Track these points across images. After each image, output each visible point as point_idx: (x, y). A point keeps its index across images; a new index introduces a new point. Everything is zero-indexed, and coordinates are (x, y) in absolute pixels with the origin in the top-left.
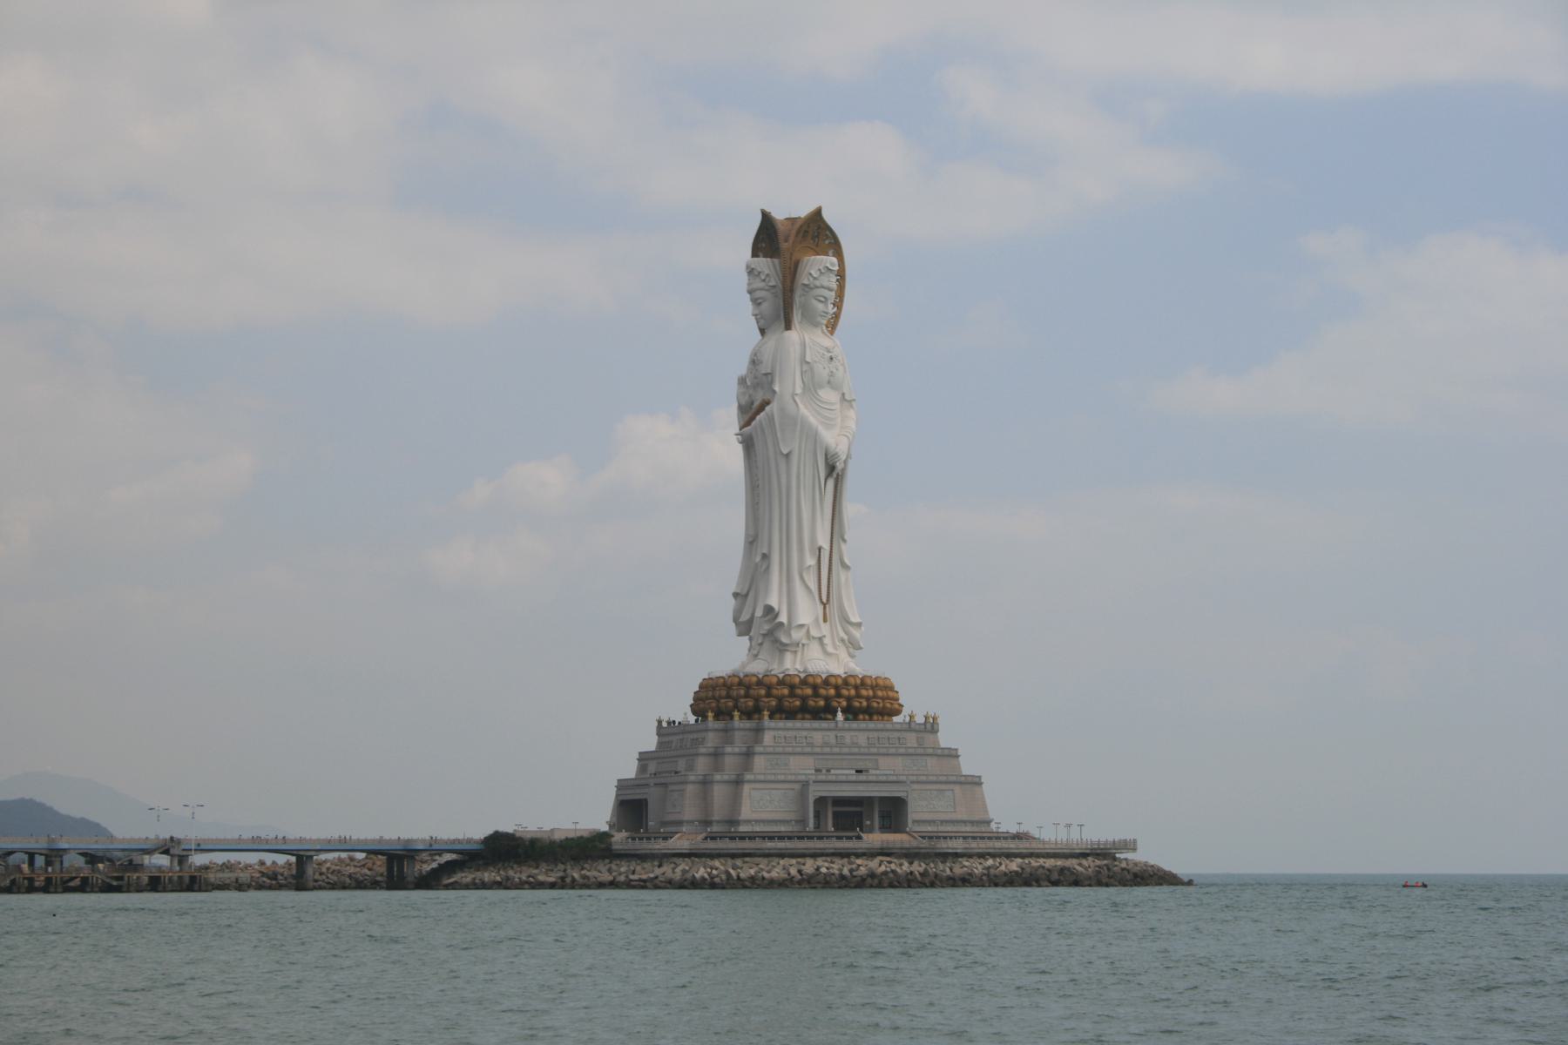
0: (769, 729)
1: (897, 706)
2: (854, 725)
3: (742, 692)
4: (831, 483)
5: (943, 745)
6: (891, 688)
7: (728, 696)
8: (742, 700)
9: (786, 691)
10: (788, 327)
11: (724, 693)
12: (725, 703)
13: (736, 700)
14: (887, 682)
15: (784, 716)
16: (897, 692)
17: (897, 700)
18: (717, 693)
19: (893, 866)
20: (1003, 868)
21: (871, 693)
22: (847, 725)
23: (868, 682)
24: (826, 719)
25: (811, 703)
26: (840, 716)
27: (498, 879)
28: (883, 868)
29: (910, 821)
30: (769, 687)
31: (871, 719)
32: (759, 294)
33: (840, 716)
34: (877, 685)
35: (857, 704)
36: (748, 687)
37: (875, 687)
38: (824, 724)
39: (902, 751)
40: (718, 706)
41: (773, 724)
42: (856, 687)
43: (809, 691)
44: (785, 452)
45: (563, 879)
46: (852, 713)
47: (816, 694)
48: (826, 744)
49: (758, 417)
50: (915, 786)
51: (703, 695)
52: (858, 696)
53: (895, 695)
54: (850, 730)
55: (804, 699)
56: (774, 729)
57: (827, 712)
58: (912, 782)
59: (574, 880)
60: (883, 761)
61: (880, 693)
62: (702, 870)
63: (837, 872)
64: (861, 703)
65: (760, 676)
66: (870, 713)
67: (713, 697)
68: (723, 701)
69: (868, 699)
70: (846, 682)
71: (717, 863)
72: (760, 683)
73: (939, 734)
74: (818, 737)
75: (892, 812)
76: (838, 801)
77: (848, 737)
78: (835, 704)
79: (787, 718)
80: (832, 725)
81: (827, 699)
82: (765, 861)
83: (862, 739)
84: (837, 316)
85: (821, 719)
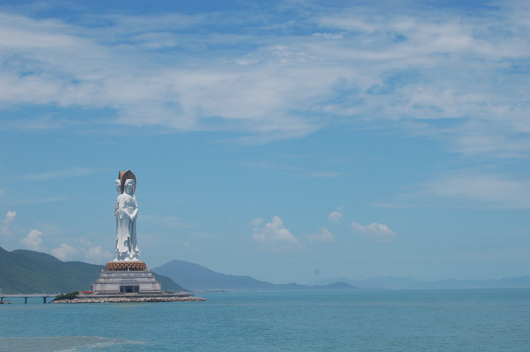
4: (131, 224)
8: (111, 267)
10: (122, 194)
13: (114, 267)
19: (125, 299)
20: (148, 300)
26: (128, 270)
27: (58, 302)
28: (123, 300)
29: (140, 291)
30: (116, 264)
32: (118, 187)
33: (128, 270)
34: (138, 263)
44: (121, 218)
45: (67, 302)
46: (131, 269)
48: (125, 276)
49: (116, 211)
50: (141, 284)
57: (126, 269)
58: (141, 283)
59: (69, 303)
60: (136, 279)
62: (90, 300)
63: (114, 301)
66: (136, 269)
70: (131, 263)
71: (93, 299)
74: (124, 275)
75: (137, 289)
76: (126, 287)
77: (130, 274)
81: (127, 266)
82: (102, 299)
83: (133, 274)
84: (135, 190)
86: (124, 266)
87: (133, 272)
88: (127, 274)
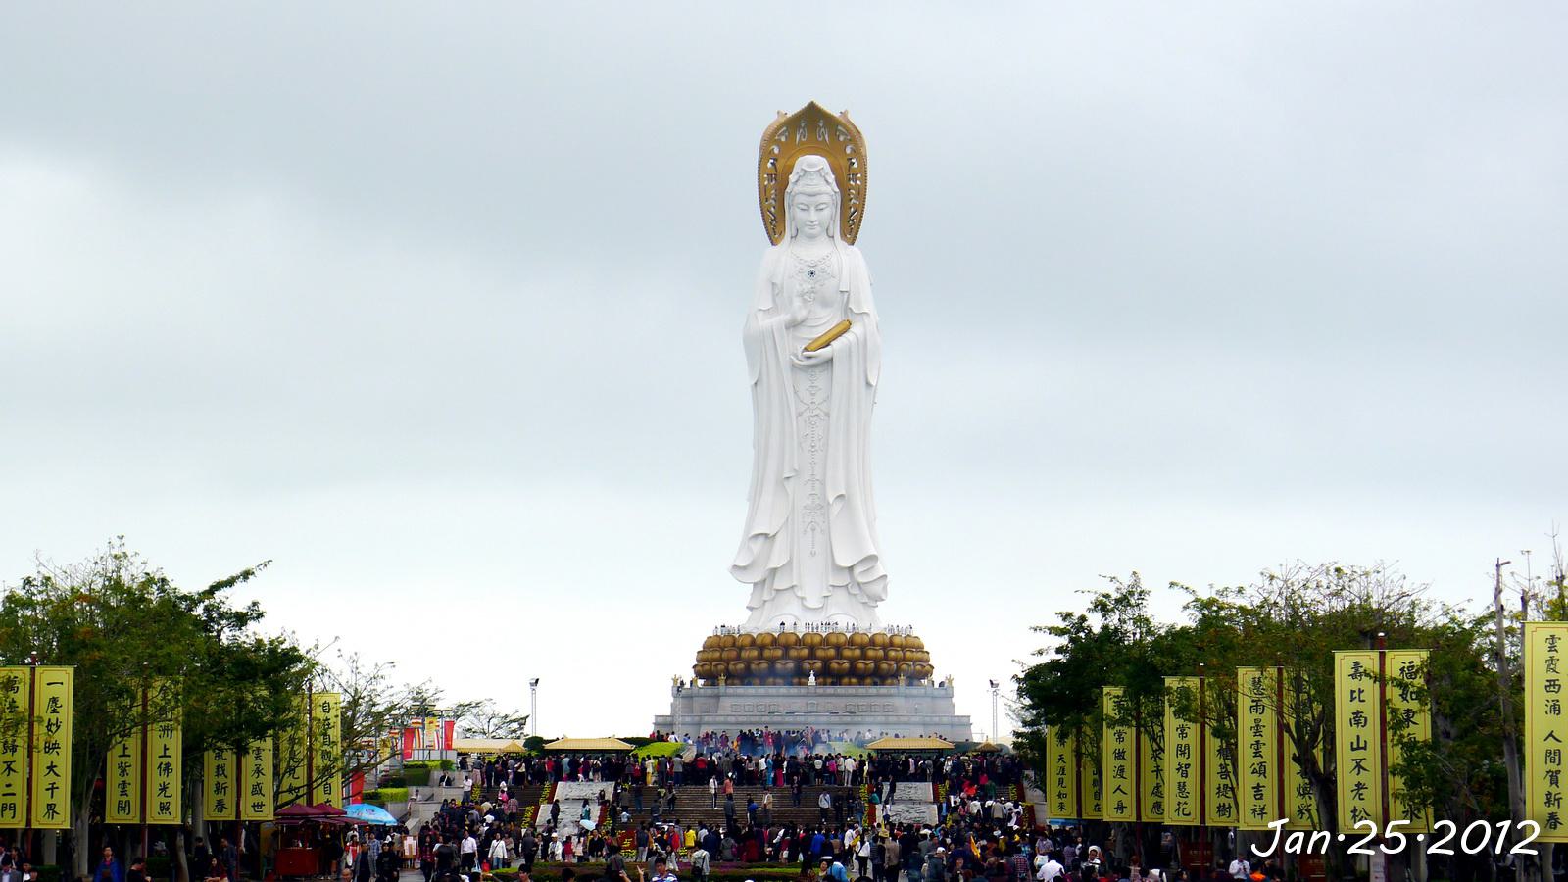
0: (726, 695)
1: (928, 668)
2: (830, 690)
3: (755, 653)
5: (957, 713)
6: (920, 648)
7: (738, 658)
8: (756, 662)
9: (779, 652)
11: (734, 654)
12: (735, 665)
14: (917, 641)
15: (829, 680)
16: (928, 653)
17: (928, 661)
18: (725, 655)
21: (900, 654)
22: (821, 690)
23: (897, 640)
24: (800, 684)
25: (834, 666)
26: (812, 679)
31: (883, 684)
33: (812, 679)
34: (891, 644)
35: (861, 666)
36: (762, 647)
37: (903, 647)
38: (794, 690)
39: (894, 719)
40: (727, 669)
41: (731, 690)
42: (863, 647)
43: (832, 652)
47: (839, 655)
51: (705, 655)
52: (886, 657)
53: (919, 655)
54: (821, 695)
55: (748, 662)
56: (730, 696)
57: (800, 675)
61: (908, 654)
64: (890, 665)
65: (755, 636)
66: (879, 677)
67: (721, 659)
68: (733, 663)
69: (877, 660)
70: (851, 642)
72: (775, 642)
73: (953, 700)
78: (806, 666)
79: (833, 684)
80: (803, 690)
85: (791, 684)
86: (785, 656)
87: (840, 690)
88: (798, 704)
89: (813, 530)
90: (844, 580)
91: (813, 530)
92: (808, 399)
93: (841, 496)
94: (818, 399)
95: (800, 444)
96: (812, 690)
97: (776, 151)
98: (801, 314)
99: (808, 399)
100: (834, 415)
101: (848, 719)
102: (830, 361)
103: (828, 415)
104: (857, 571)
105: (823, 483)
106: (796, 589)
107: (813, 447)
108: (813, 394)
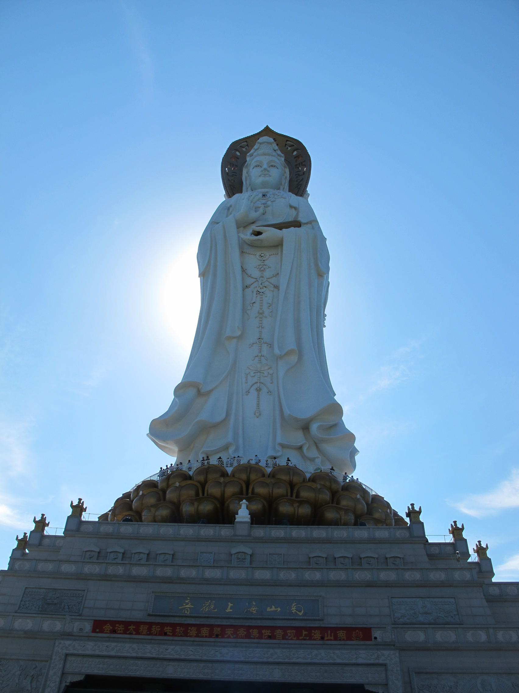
22: (260, 531)
80: (225, 531)
89: (259, 390)
90: (298, 438)
91: (259, 390)
92: (256, 273)
93: (290, 353)
94: (268, 273)
95: (244, 310)
96: (242, 531)
97: (238, 153)
98: (254, 215)
99: (256, 273)
100: (283, 288)
101: (318, 576)
102: (278, 245)
103: (277, 287)
104: (314, 428)
105: (271, 346)
106: (231, 449)
107: (261, 314)
108: (262, 270)
